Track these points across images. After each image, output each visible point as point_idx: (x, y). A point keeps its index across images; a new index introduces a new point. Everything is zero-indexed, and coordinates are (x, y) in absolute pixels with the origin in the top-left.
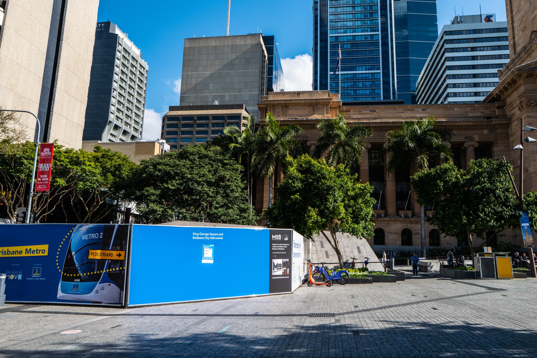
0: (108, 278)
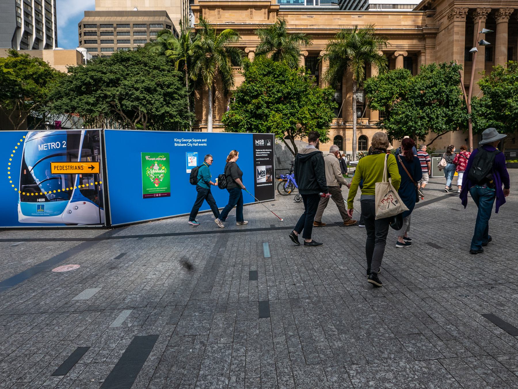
0: (82, 196)
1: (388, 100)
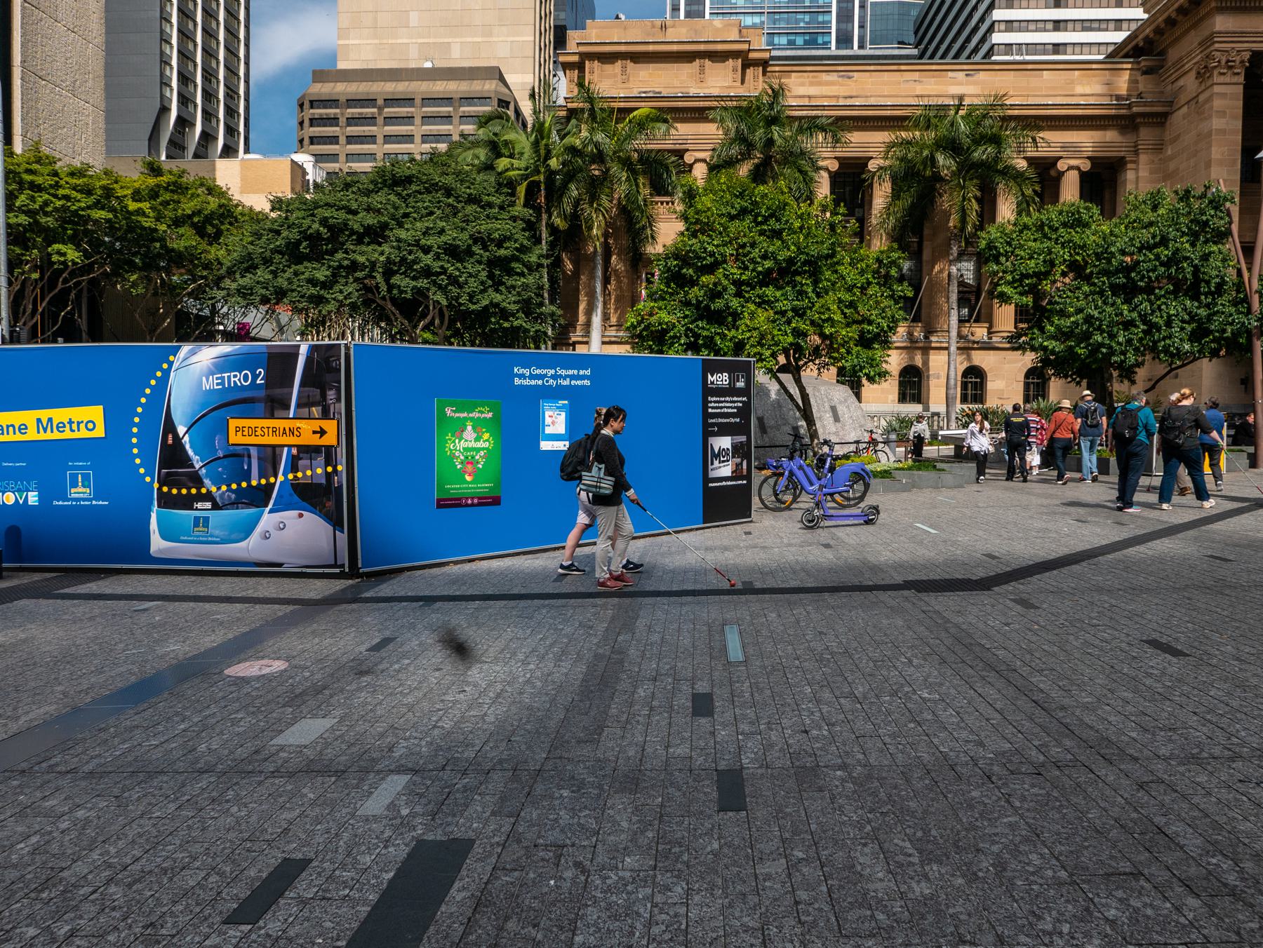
0: (296, 498)
1: (1040, 280)
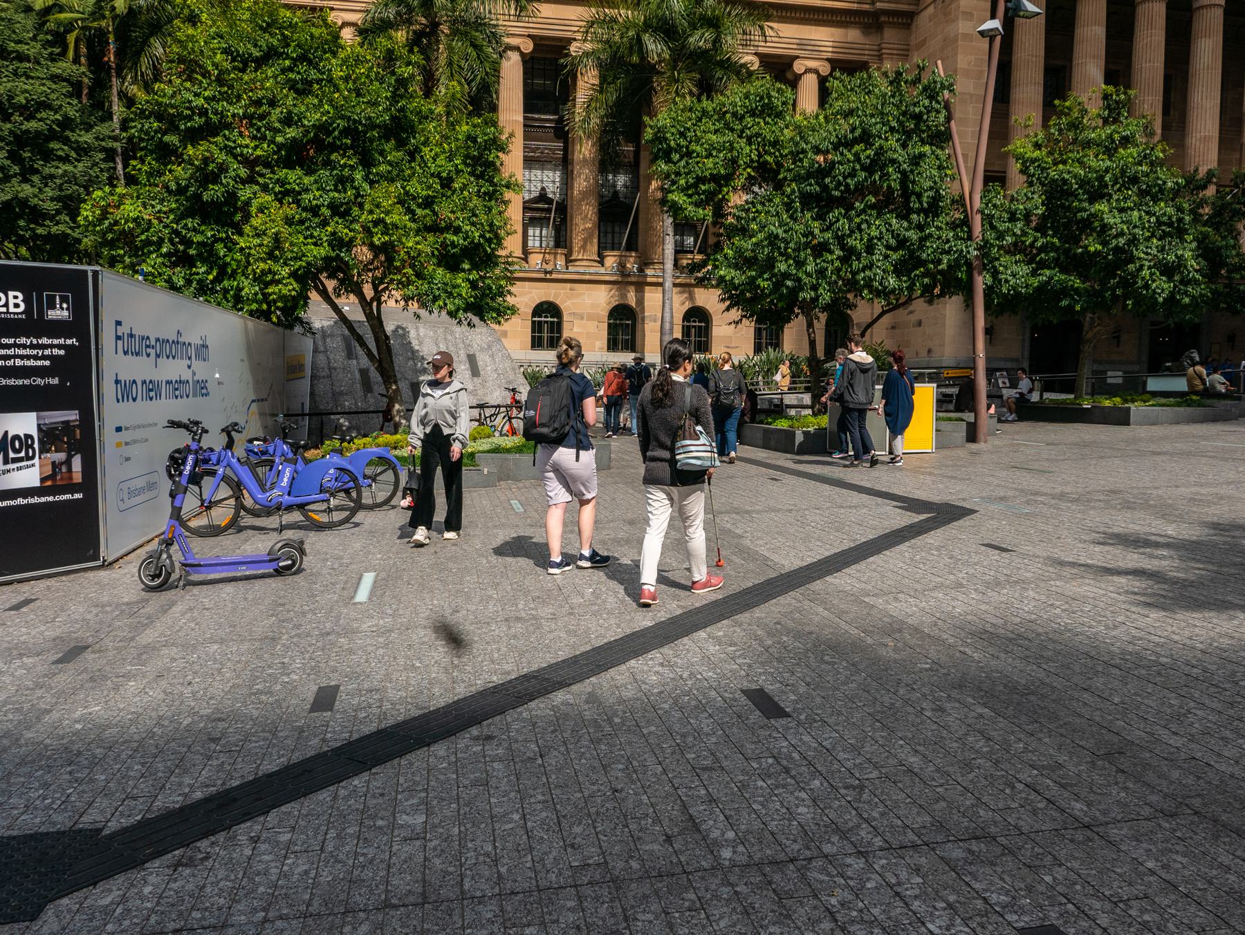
1: (721, 186)
